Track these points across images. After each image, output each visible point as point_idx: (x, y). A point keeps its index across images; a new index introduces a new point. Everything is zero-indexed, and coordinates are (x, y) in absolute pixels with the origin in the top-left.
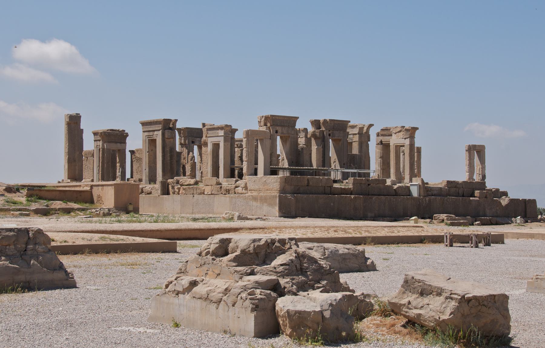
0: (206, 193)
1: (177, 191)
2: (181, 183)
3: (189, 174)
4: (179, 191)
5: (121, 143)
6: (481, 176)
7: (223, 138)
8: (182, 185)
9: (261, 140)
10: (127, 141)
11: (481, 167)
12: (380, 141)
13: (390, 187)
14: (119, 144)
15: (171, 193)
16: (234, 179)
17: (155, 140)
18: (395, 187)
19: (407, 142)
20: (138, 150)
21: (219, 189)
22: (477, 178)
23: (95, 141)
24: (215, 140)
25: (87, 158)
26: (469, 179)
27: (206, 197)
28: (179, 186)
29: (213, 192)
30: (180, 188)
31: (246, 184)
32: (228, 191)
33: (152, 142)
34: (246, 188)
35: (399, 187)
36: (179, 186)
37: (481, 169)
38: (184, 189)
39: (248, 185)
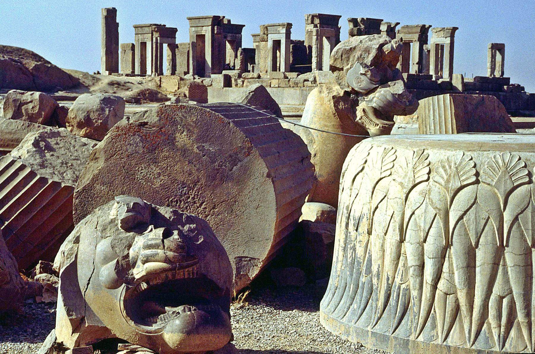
0: (272, 86)
1: (241, 83)
2: (244, 76)
3: (238, 68)
4: (243, 83)
5: (172, 38)
6: (500, 72)
7: (285, 34)
8: (245, 78)
9: (328, 38)
10: (176, 36)
11: (500, 64)
12: (400, 38)
13: (436, 82)
14: (170, 39)
15: (233, 85)
16: (297, 73)
17: (204, 35)
18: (440, 81)
19: (448, 40)
20: (181, 45)
21: (287, 83)
22: (497, 74)
23: (136, 34)
24: (276, 37)
25: (125, 51)
26: (491, 75)
27: (275, 89)
28: (243, 80)
29: (280, 86)
30: (244, 81)
31: (315, 78)
32: (296, 84)
33: (201, 38)
34: (315, 81)
35: (443, 82)
36: (243, 80)
37: (500, 66)
38: (248, 82)
39: (317, 79)
